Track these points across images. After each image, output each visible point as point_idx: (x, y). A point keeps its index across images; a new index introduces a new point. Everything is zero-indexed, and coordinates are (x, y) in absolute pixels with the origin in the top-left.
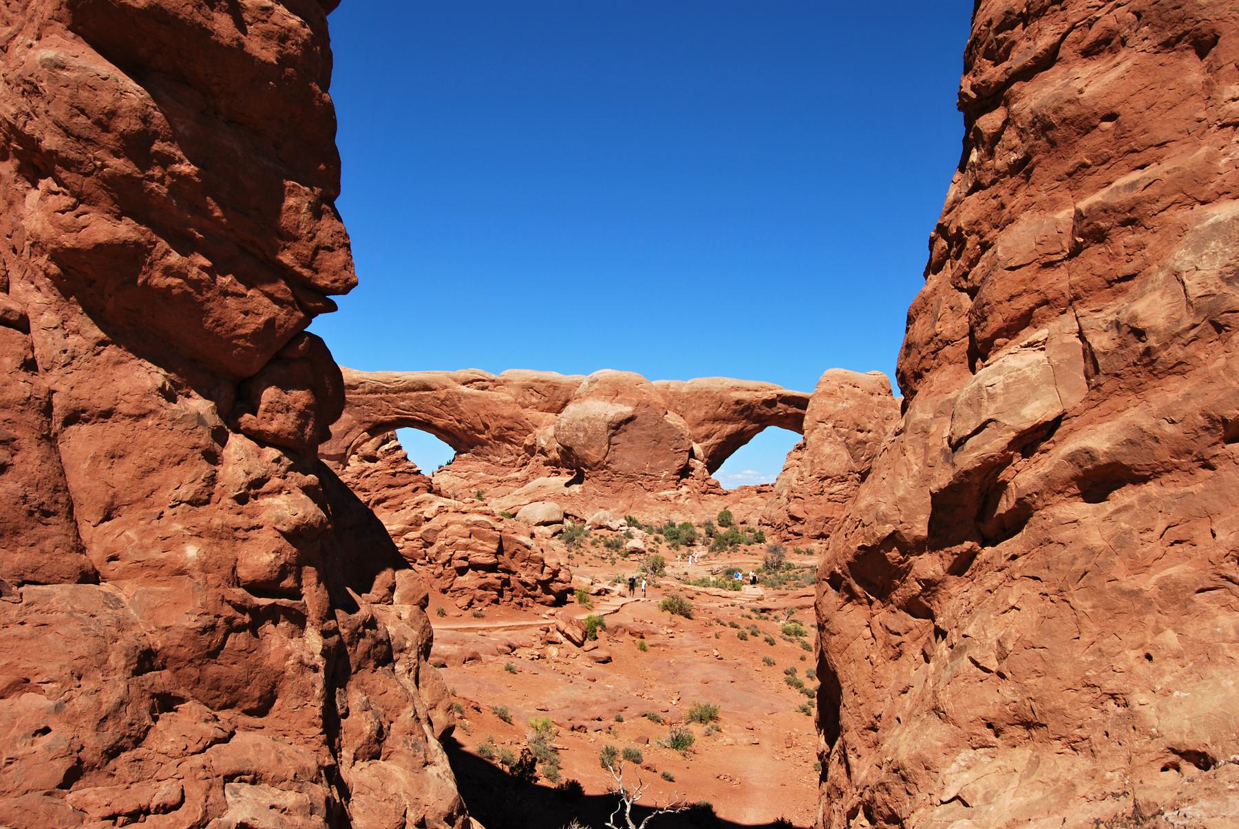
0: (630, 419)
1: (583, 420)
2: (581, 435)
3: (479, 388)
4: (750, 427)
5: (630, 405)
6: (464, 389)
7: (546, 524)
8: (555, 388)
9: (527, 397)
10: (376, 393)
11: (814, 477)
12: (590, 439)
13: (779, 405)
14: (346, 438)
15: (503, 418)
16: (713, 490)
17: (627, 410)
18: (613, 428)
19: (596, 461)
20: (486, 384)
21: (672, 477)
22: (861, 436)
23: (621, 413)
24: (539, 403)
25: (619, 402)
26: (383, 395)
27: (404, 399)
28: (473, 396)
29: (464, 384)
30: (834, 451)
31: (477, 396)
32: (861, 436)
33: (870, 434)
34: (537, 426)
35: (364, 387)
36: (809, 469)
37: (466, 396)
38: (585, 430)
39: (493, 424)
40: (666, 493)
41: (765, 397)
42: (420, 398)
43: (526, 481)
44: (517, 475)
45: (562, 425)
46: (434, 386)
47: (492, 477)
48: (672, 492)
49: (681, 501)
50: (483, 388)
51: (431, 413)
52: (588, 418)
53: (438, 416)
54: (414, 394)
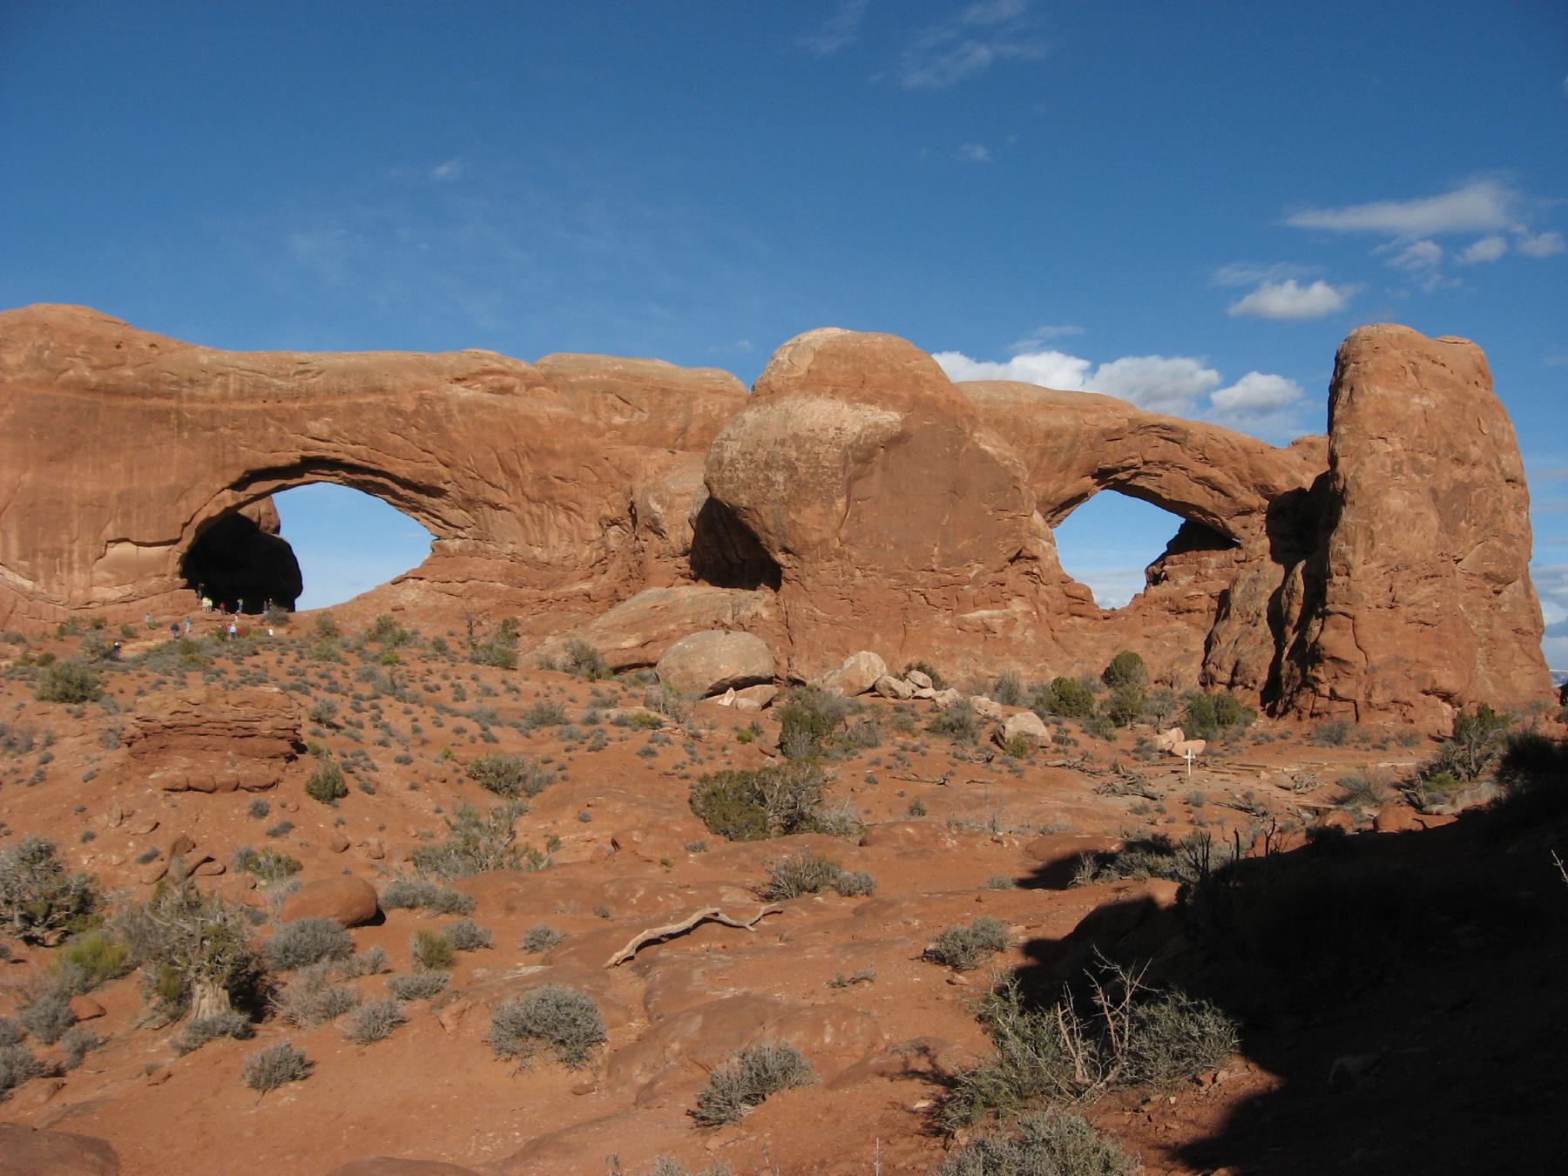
0: (895, 441)
1: (783, 443)
2: (780, 477)
3: (492, 390)
4: (1070, 490)
5: (896, 408)
6: (461, 392)
7: (740, 684)
8: (665, 392)
9: (603, 413)
10: (253, 397)
11: (1374, 565)
12: (801, 485)
13: (1134, 440)
14: (183, 503)
15: (552, 454)
16: (1081, 609)
17: (890, 418)
18: (857, 461)
19: (815, 537)
20: (508, 380)
21: (991, 577)
22: (1460, 473)
23: (876, 425)
24: (627, 424)
25: (870, 402)
26: (270, 405)
27: (317, 414)
28: (481, 406)
29: (458, 380)
30: (1412, 505)
31: (491, 408)
32: (1460, 473)
33: (1477, 472)
34: (629, 477)
35: (225, 386)
36: (1361, 545)
37: (465, 407)
38: (790, 467)
39: (528, 469)
40: (984, 613)
41: (1104, 424)
42: (356, 410)
43: (616, 599)
44: (586, 586)
45: (727, 455)
46: (389, 384)
47: (525, 591)
48: (996, 612)
49: (1016, 634)
50: (504, 390)
51: (376, 444)
52: (795, 436)
53: (395, 452)
54: (341, 403)
